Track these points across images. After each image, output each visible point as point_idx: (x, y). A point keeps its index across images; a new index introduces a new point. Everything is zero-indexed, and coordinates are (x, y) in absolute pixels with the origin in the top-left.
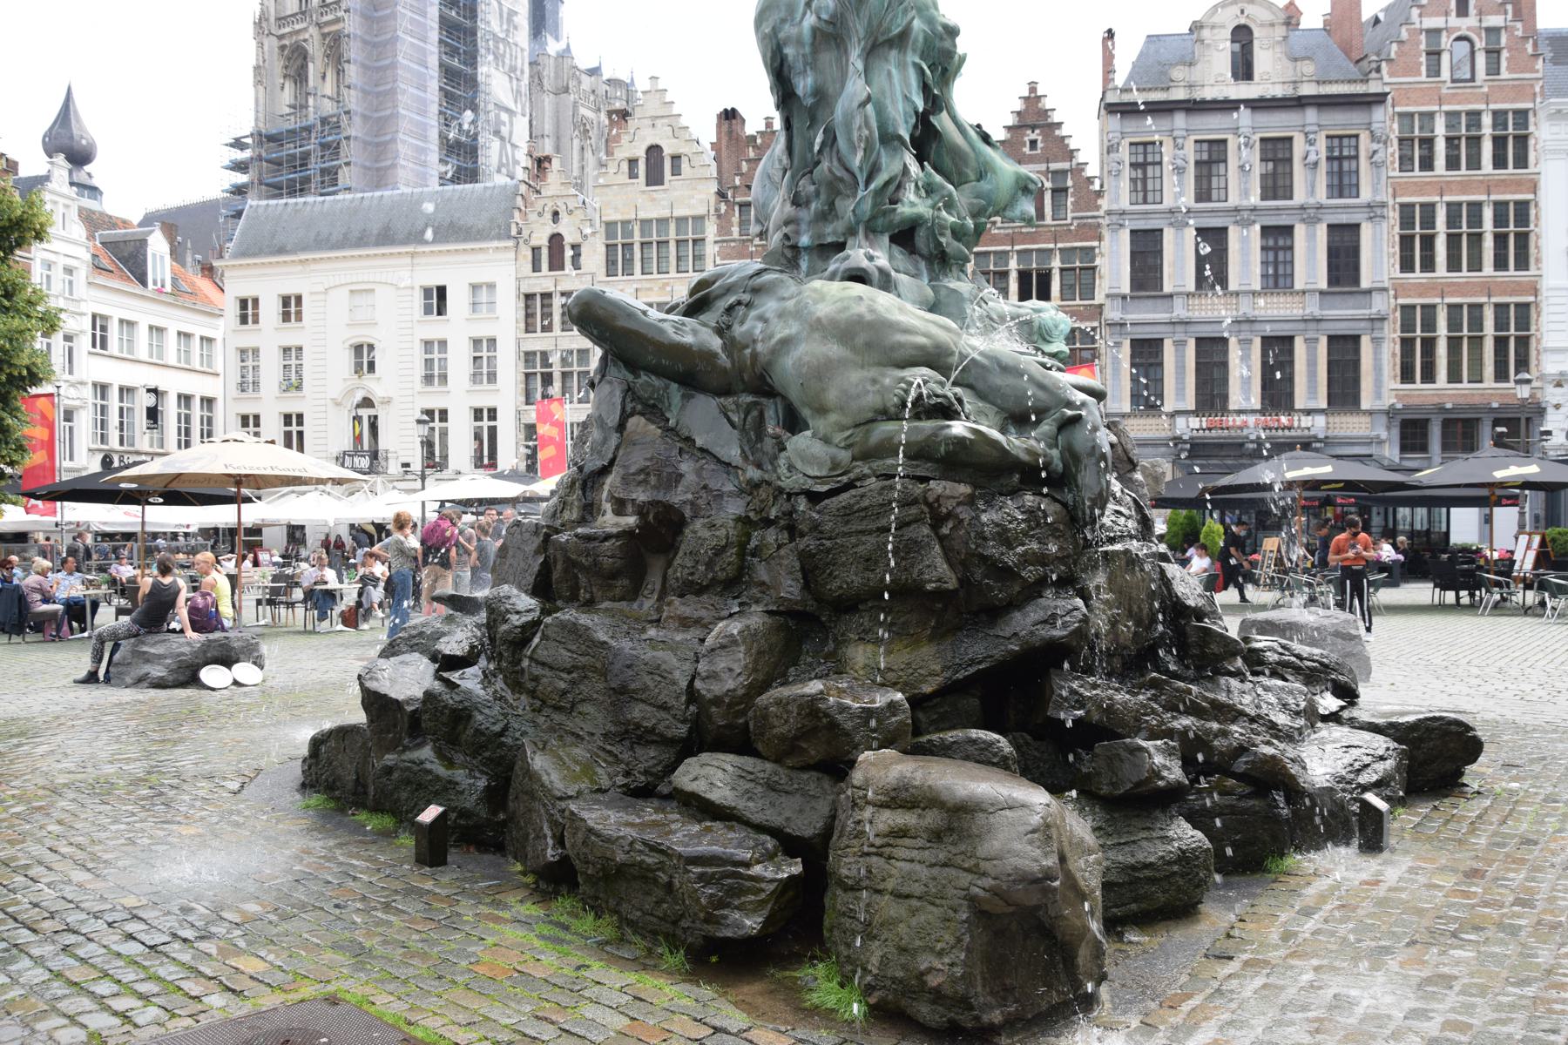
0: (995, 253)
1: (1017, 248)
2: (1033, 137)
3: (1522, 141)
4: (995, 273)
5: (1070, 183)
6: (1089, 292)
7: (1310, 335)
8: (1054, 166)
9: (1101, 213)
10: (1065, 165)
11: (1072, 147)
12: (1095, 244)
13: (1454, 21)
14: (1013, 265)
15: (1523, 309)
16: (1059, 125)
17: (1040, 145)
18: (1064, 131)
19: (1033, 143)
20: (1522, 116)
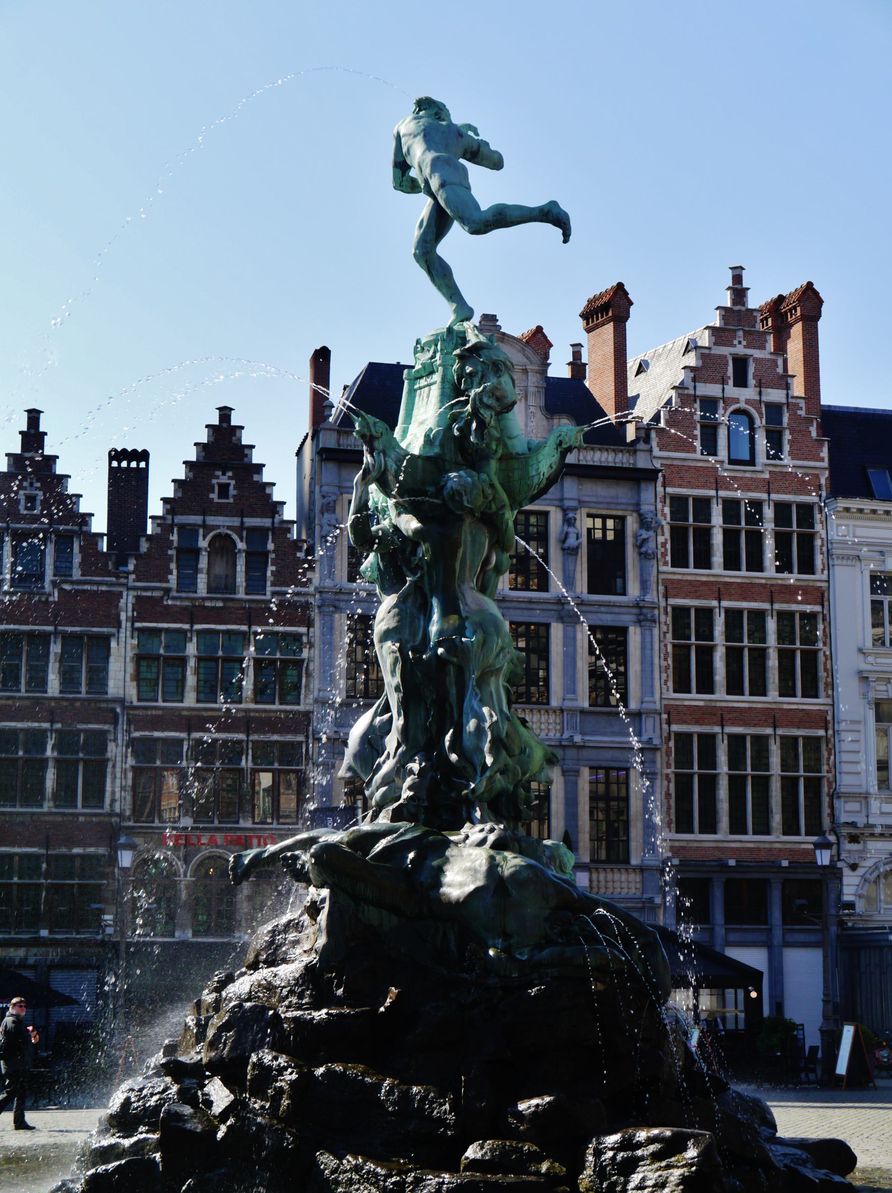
0: (167, 630)
1: (197, 627)
2: (224, 480)
3: (807, 542)
4: (166, 658)
5: (271, 546)
6: (292, 692)
7: (570, 764)
8: (250, 522)
9: (311, 589)
10: (266, 522)
11: (276, 498)
12: (303, 630)
13: (731, 391)
14: (191, 649)
15: (813, 744)
16: (260, 467)
17: (232, 491)
18: (266, 477)
19: (224, 490)
20: (806, 512)
